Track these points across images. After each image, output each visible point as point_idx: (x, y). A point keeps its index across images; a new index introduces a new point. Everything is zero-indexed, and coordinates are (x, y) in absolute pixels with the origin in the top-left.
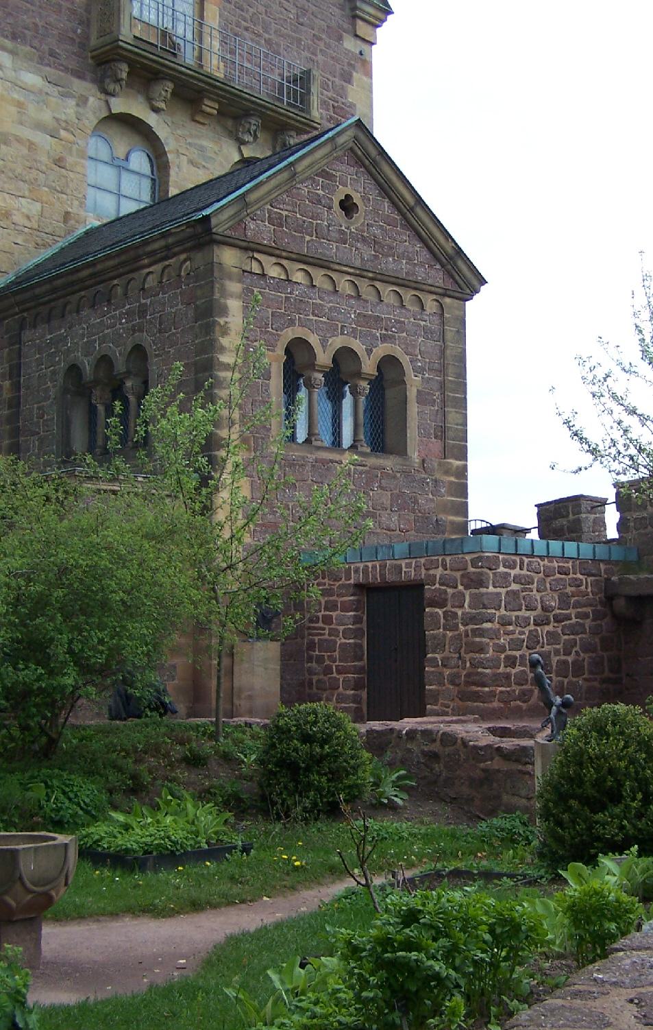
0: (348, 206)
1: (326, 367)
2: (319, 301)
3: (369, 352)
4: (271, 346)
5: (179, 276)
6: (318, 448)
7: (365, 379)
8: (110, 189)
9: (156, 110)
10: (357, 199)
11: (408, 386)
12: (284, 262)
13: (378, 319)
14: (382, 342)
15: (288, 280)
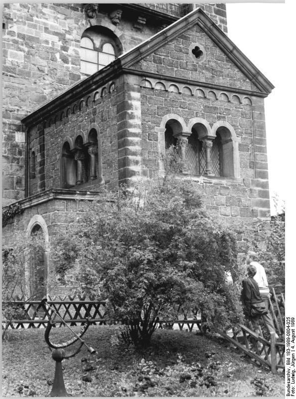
0: (197, 52)
1: (189, 134)
2: (183, 101)
3: (211, 125)
4: (158, 124)
5: (110, 92)
6: (186, 175)
7: (210, 139)
8: (92, 59)
9: (115, 24)
10: (202, 48)
11: (233, 142)
12: (163, 81)
13: (215, 108)
14: (219, 120)
15: (167, 91)
